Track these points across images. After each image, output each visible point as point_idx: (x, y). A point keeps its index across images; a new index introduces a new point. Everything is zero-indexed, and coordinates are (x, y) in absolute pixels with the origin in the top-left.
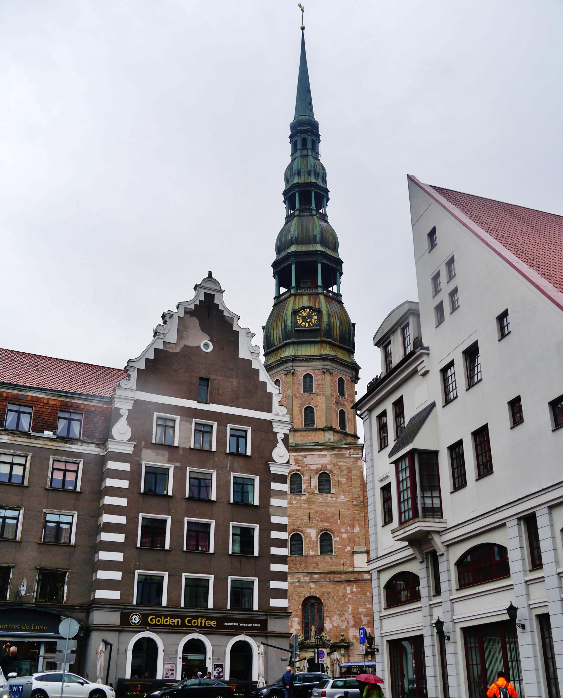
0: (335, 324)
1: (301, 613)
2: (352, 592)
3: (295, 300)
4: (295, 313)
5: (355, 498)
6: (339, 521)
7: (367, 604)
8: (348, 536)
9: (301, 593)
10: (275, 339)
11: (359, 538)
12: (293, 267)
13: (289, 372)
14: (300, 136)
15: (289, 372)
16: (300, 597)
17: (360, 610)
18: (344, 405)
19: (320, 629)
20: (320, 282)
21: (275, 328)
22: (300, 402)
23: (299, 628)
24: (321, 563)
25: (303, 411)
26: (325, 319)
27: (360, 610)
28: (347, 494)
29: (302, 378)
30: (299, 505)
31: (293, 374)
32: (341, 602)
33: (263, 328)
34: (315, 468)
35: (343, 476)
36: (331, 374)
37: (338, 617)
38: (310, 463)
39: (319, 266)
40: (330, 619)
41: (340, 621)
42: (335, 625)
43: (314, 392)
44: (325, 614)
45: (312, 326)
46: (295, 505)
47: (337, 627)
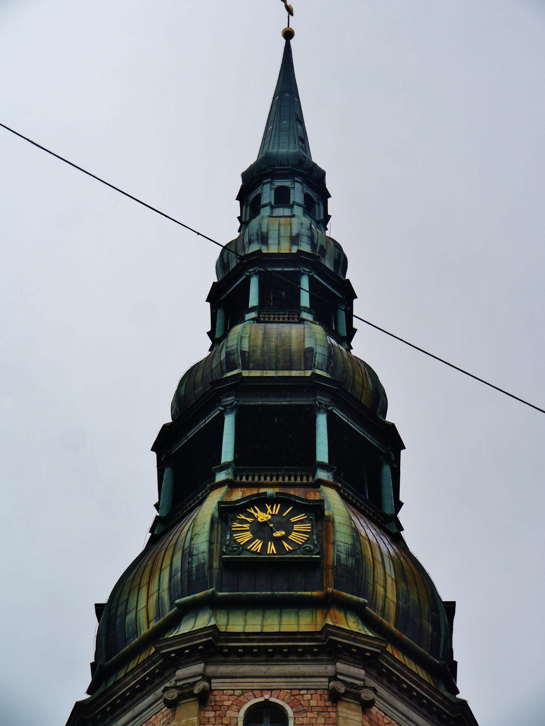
0: (379, 568)
3: (229, 493)
4: (226, 513)
10: (142, 615)
12: (229, 421)
13: (185, 693)
14: (271, 183)
15: (185, 693)
20: (322, 454)
21: (145, 580)
26: (342, 537)
29: (242, 714)
31: (204, 699)
33: (99, 608)
36: (366, 706)
39: (322, 421)
45: (290, 552)
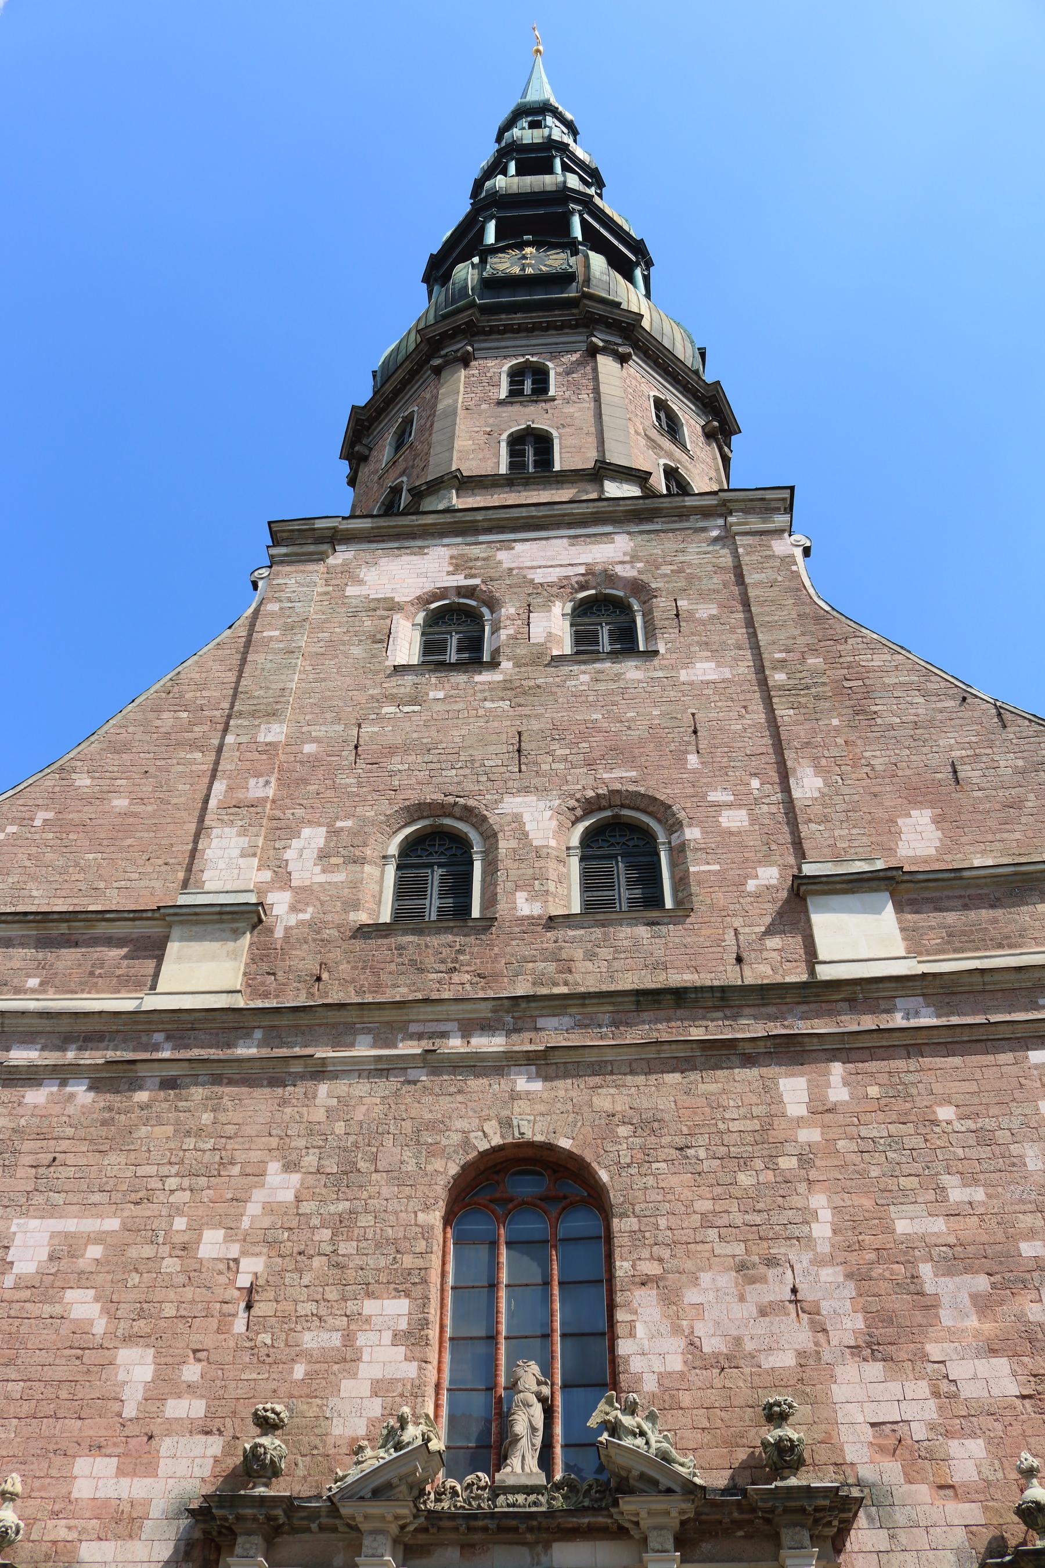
1: (436, 1261)
2: (821, 1110)
5: (781, 665)
6: (693, 760)
7: (949, 1181)
8: (754, 820)
9: (438, 1126)
11: (825, 819)
16: (434, 1151)
17: (902, 1227)
18: (680, 462)
19: (594, 1366)
22: (491, 421)
23: (411, 1370)
24: (590, 956)
25: (505, 436)
27: (902, 1227)
28: (732, 653)
29: (505, 368)
30: (461, 706)
32: (744, 1179)
34: (553, 579)
35: (703, 596)
37: (727, 1280)
38: (529, 564)
40: (670, 1299)
41: (750, 1309)
42: (712, 1345)
43: (552, 393)
44: (622, 1267)
46: (439, 707)
47: (726, 1363)
